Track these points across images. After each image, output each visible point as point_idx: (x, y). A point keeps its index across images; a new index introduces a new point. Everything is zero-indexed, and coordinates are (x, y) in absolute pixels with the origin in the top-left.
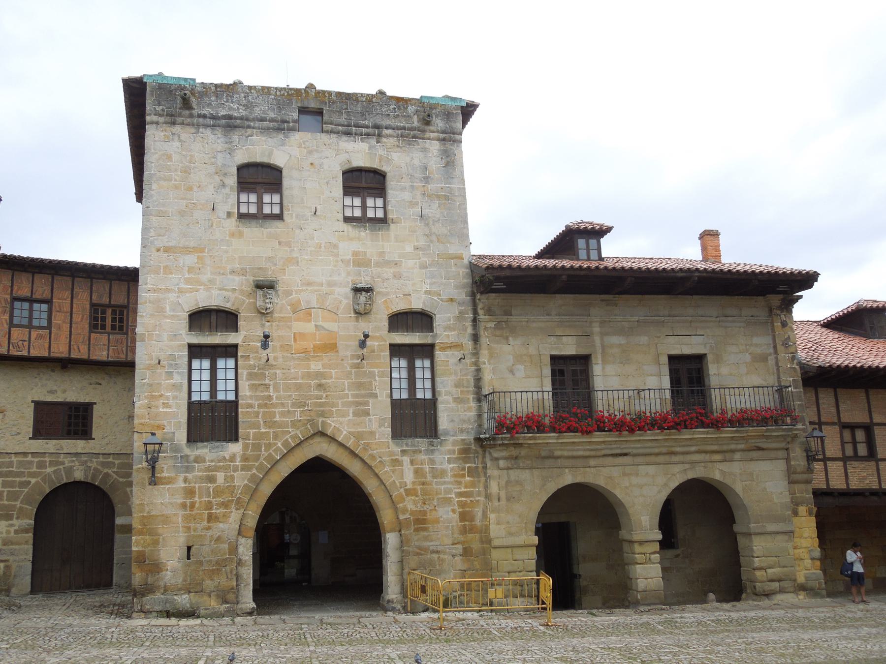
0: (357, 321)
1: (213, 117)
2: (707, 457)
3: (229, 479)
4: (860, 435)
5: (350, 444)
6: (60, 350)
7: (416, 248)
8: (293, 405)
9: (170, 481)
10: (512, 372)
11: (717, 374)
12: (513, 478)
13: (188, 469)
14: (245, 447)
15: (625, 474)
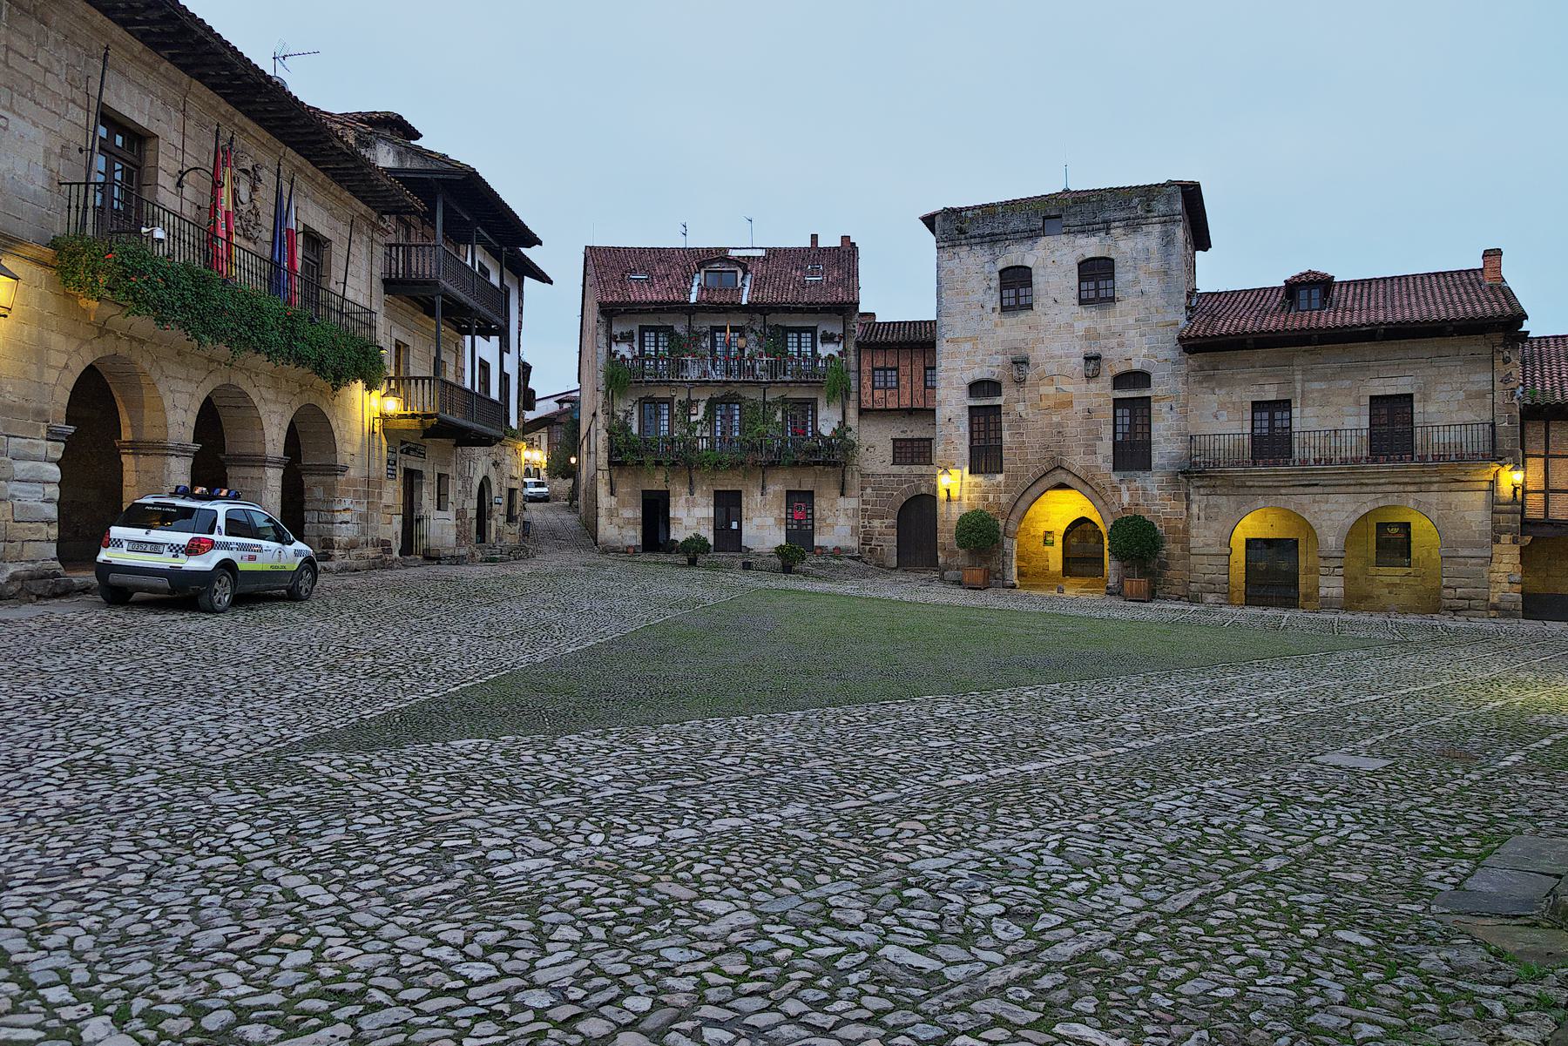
1: (982, 237)
2: (1401, 488)
6: (906, 402)
11: (1423, 412)
14: (1007, 477)
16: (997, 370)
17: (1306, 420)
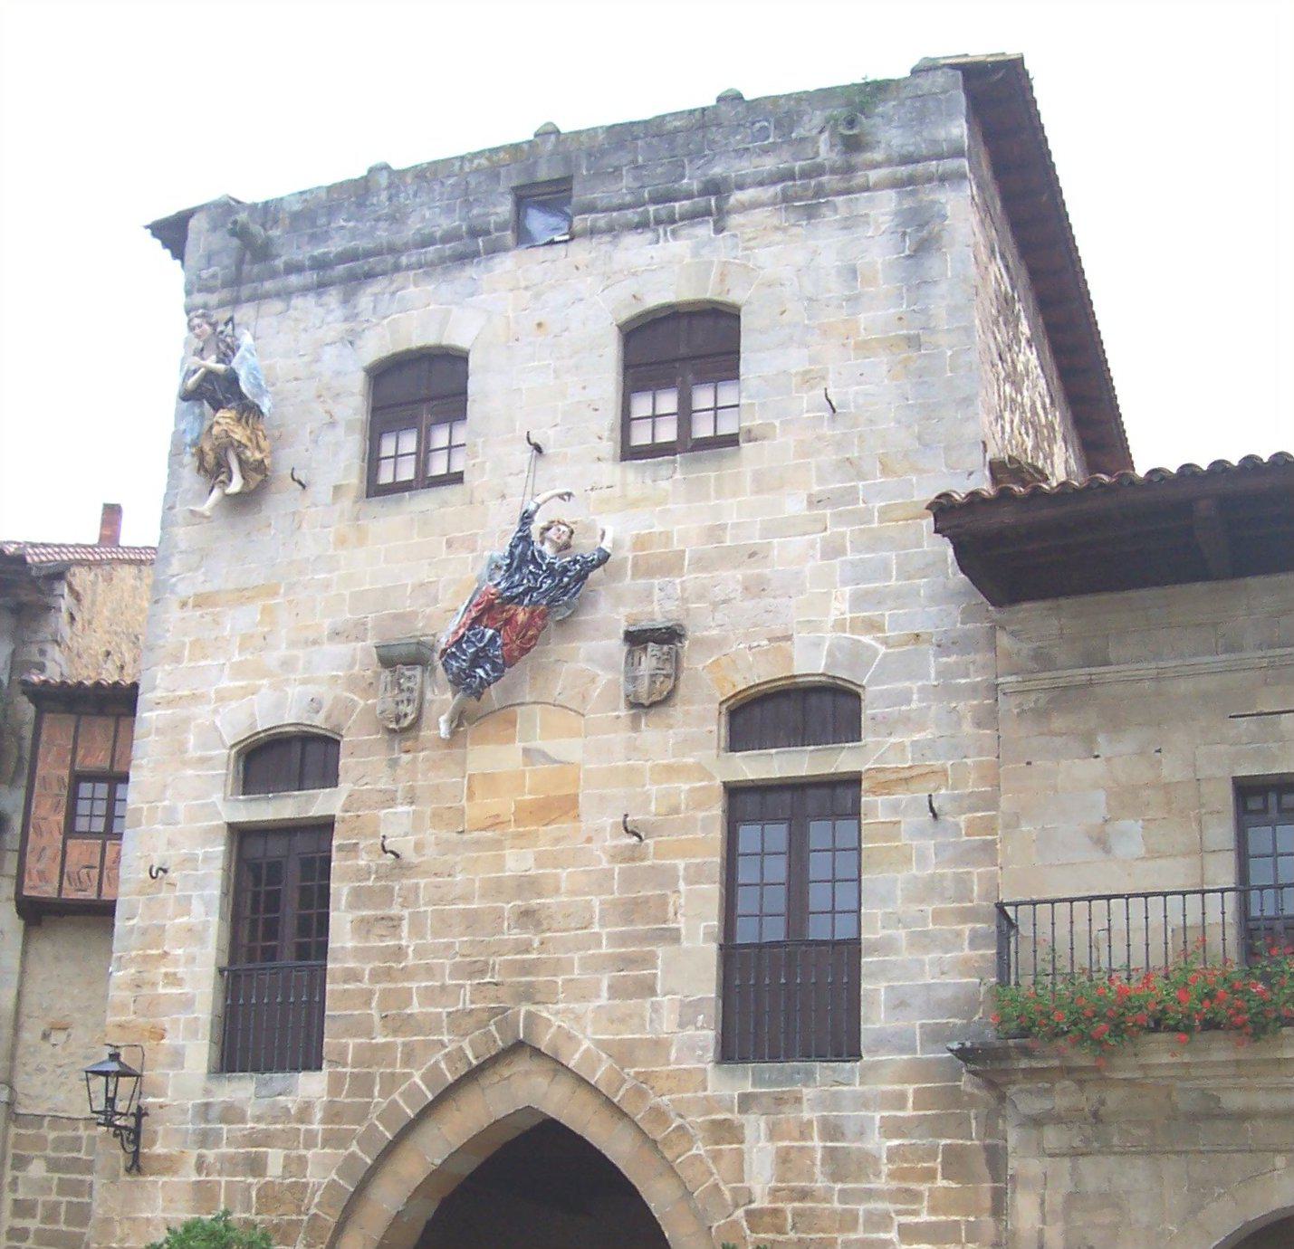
0: (635, 725)
1: (320, 264)
3: (294, 1167)
5: (598, 1076)
7: (815, 502)
8: (457, 971)
9: (169, 1165)
10: (1101, 842)
12: (1091, 1184)
13: (205, 1139)
14: (336, 1083)
16: (328, 695)
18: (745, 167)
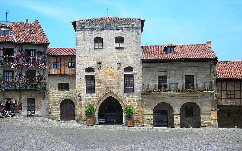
1: (89, 28)
2: (192, 97)
4: (232, 93)
6: (63, 73)
15: (173, 101)
17: (171, 81)
18: (124, 26)
